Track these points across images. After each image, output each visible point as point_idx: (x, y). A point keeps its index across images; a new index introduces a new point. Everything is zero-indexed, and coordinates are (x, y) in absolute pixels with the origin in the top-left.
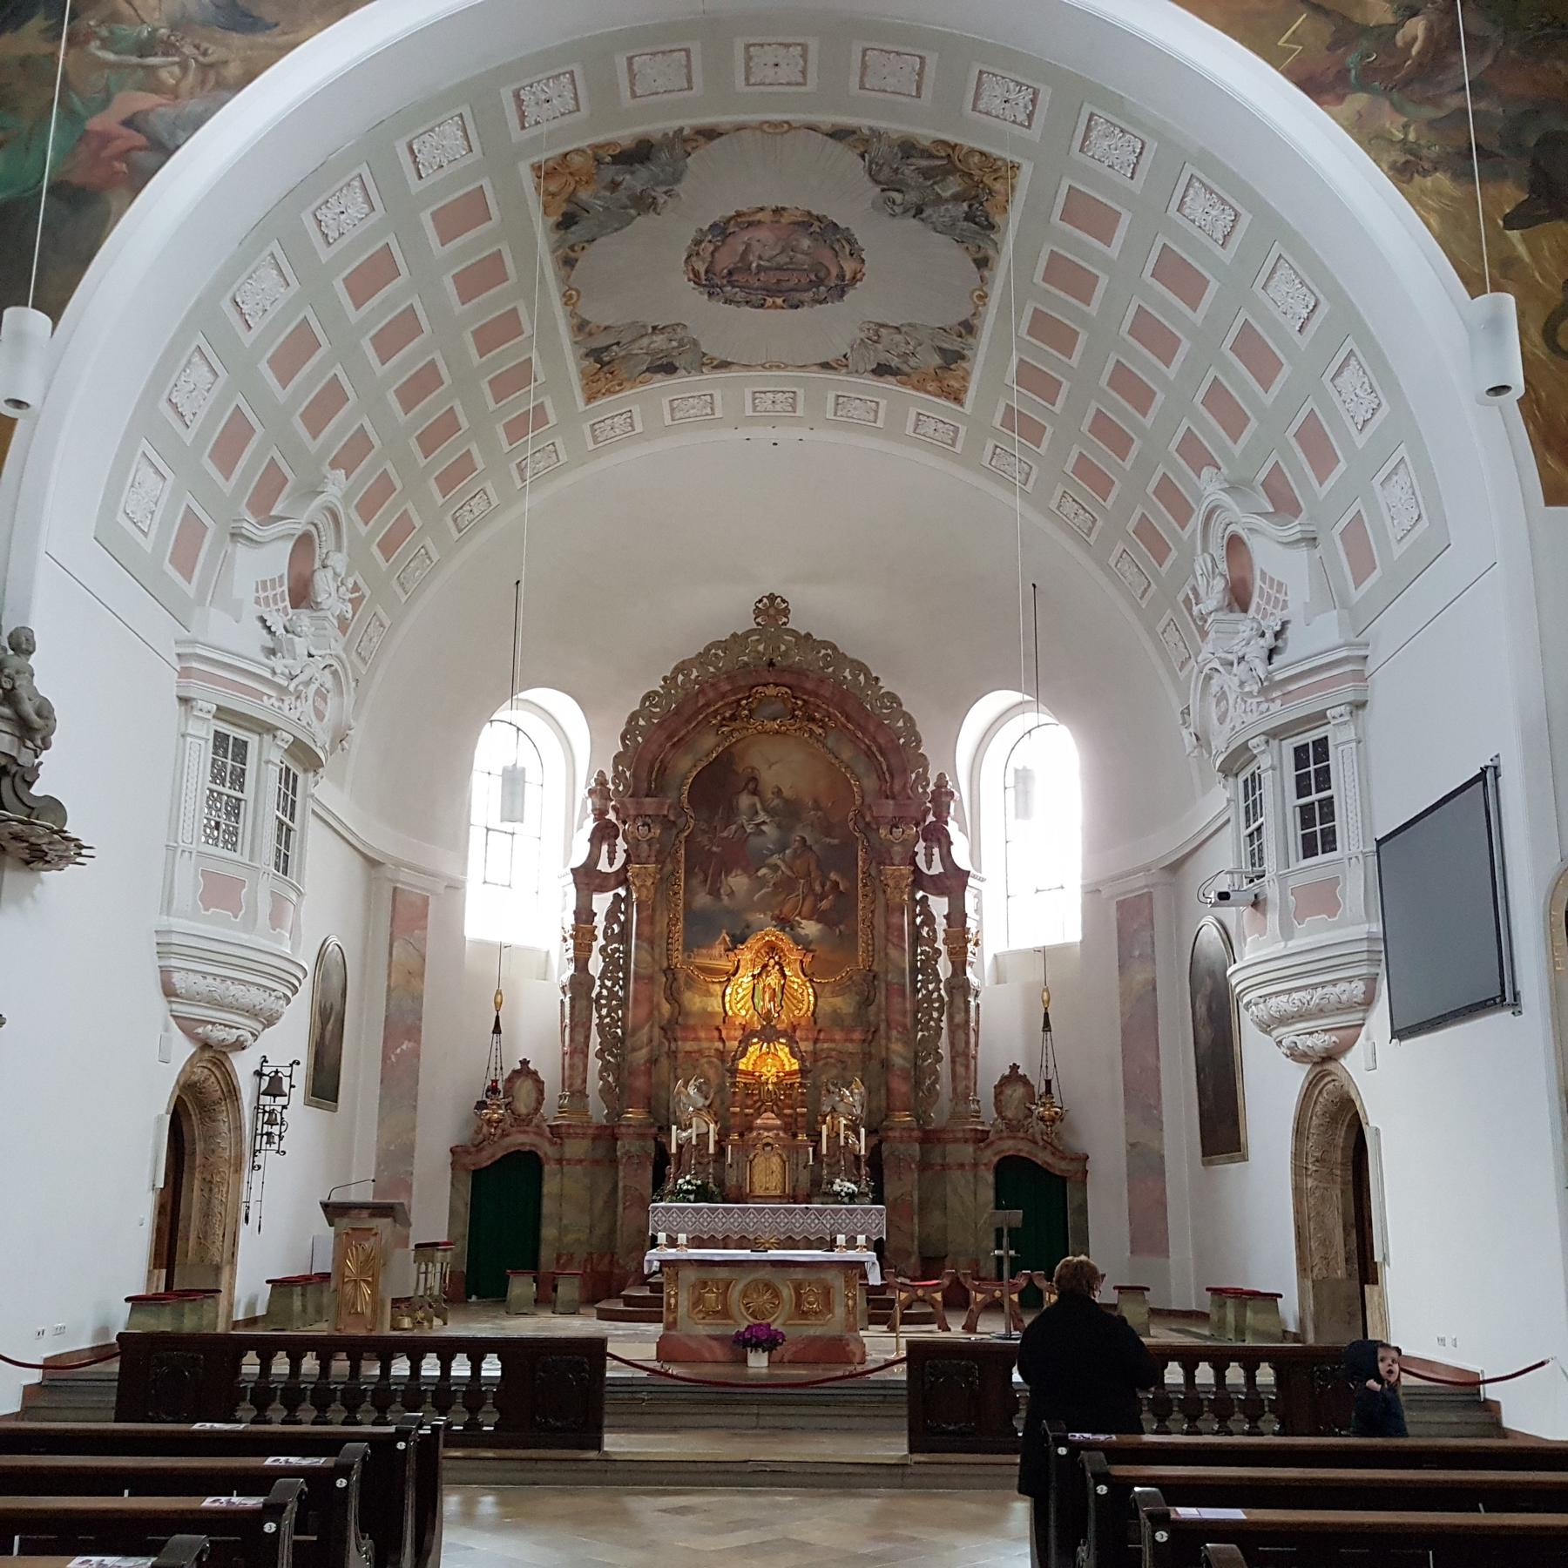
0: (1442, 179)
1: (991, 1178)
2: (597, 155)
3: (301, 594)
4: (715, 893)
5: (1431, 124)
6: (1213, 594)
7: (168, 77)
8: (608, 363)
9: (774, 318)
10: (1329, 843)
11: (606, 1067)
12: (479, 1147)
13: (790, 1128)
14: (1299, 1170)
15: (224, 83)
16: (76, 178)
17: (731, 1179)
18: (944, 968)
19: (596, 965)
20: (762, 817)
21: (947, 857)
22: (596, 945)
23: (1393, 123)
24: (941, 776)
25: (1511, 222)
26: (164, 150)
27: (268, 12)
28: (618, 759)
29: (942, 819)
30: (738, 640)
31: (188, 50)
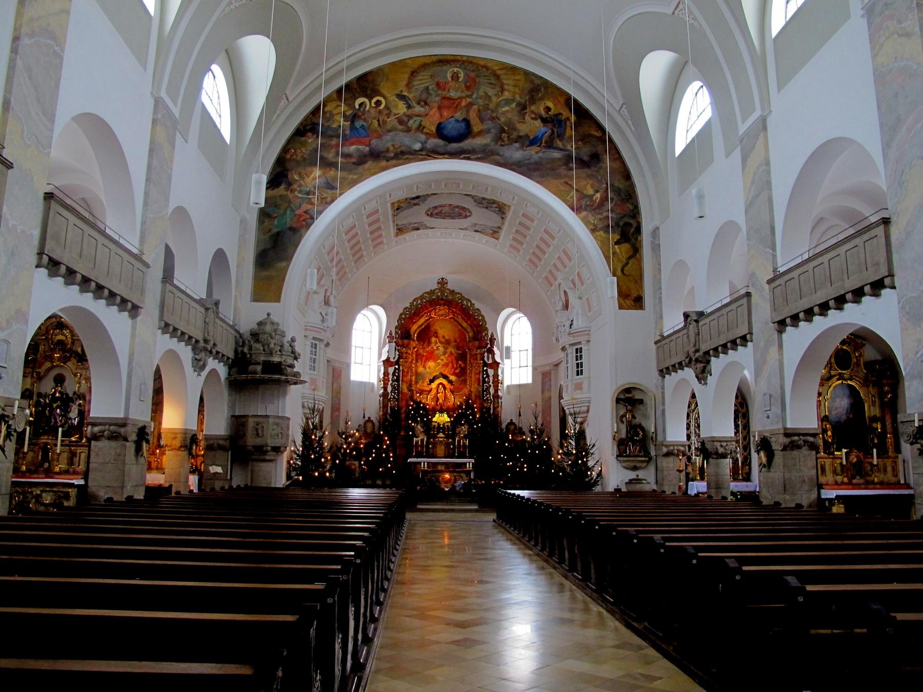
0: (601, 233)
2: (406, 199)
3: (327, 302)
4: (424, 367)
5: (600, 219)
6: (560, 305)
8: (400, 230)
9: (448, 222)
10: (582, 374)
13: (447, 437)
15: (327, 202)
16: (294, 225)
18: (492, 390)
19: (389, 389)
20: (439, 344)
21: (493, 358)
23: (591, 219)
24: (492, 335)
25: (617, 243)
28: (396, 328)
29: (492, 345)
30: (432, 292)
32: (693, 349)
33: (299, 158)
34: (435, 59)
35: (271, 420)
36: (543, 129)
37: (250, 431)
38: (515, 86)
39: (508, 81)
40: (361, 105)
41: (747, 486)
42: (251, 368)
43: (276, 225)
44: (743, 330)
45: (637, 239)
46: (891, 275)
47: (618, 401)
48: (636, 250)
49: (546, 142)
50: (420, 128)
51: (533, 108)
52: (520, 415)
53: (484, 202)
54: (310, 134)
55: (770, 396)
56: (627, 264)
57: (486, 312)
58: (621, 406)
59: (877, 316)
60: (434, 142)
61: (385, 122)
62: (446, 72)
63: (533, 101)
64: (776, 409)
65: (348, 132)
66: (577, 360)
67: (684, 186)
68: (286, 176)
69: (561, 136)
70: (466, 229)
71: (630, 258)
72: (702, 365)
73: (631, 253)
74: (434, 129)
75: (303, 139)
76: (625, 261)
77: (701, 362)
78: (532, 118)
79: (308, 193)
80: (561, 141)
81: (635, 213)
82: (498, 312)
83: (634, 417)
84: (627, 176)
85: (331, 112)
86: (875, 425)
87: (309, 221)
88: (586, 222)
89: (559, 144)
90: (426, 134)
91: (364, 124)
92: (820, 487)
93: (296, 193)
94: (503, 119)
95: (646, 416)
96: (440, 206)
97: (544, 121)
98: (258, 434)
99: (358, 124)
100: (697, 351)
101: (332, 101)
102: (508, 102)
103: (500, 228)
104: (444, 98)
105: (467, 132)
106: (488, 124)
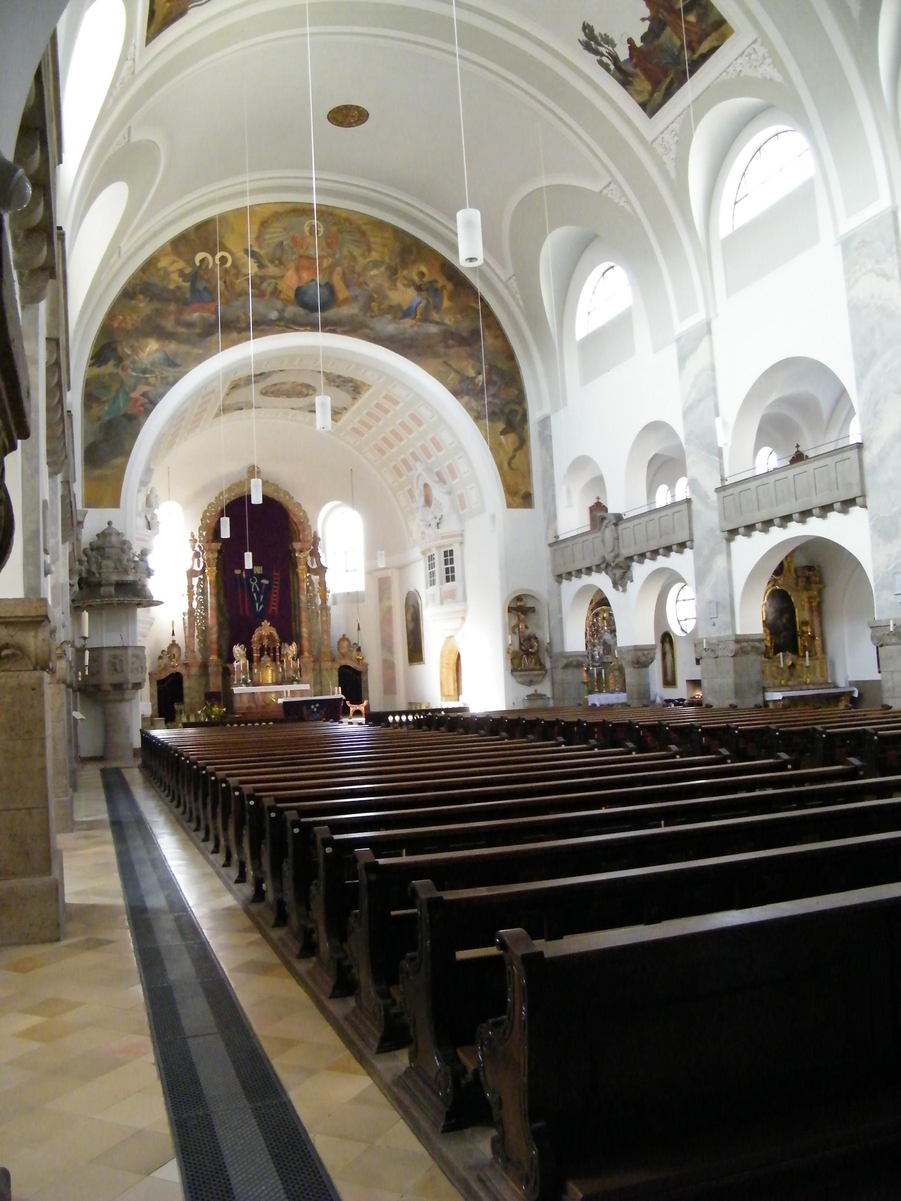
1: (336, 673)
7: (152, 380)
10: (453, 579)
11: (200, 641)
12: (160, 672)
14: (442, 667)
16: (129, 412)
17: (255, 678)
21: (318, 562)
22: (195, 597)
23: (474, 404)
24: (315, 533)
25: (502, 433)
26: (153, 403)
27: (178, 361)
28: (200, 529)
31: (157, 373)
32: (612, 555)
33: (129, 327)
34: (289, 207)
35: (130, 652)
36: (418, 299)
37: (106, 667)
38: (384, 245)
39: (376, 239)
40: (203, 261)
41: (617, 698)
42: (103, 590)
43: (105, 411)
44: (682, 537)
45: (523, 428)
46: (863, 495)
47: (510, 610)
48: (523, 442)
49: (421, 314)
50: (276, 293)
51: (405, 273)
52: (359, 629)
53: (338, 380)
54: (141, 297)
55: (718, 604)
56: (513, 457)
57: (307, 507)
58: (512, 615)
59: (844, 530)
60: (293, 310)
61: (233, 285)
62: (303, 224)
63: (404, 264)
64: (724, 617)
65: (188, 295)
66: (446, 563)
67: (589, 375)
68: (114, 350)
69: (437, 308)
70: (300, 409)
71: (516, 450)
72: (622, 571)
73: (517, 444)
74: (292, 295)
75: (133, 302)
76: (511, 453)
77: (621, 567)
78: (405, 285)
79: (144, 371)
80: (437, 312)
81: (521, 398)
82: (319, 508)
83: (526, 627)
84: (511, 356)
85: (165, 269)
86: (804, 628)
87: (149, 406)
88: (469, 409)
89: (436, 317)
90: (283, 300)
91: (207, 285)
92: (764, 690)
93: (129, 371)
94: (372, 285)
95: (539, 626)
96: (283, 383)
97: (419, 289)
98: (116, 670)
99: (200, 285)
100: (617, 556)
101: (166, 255)
102: (376, 264)
103: (345, 409)
104: (302, 257)
105: (331, 299)
106: (357, 291)
